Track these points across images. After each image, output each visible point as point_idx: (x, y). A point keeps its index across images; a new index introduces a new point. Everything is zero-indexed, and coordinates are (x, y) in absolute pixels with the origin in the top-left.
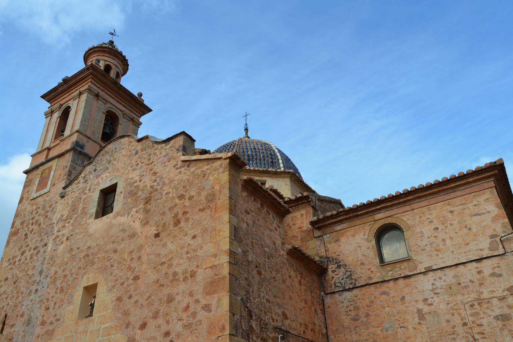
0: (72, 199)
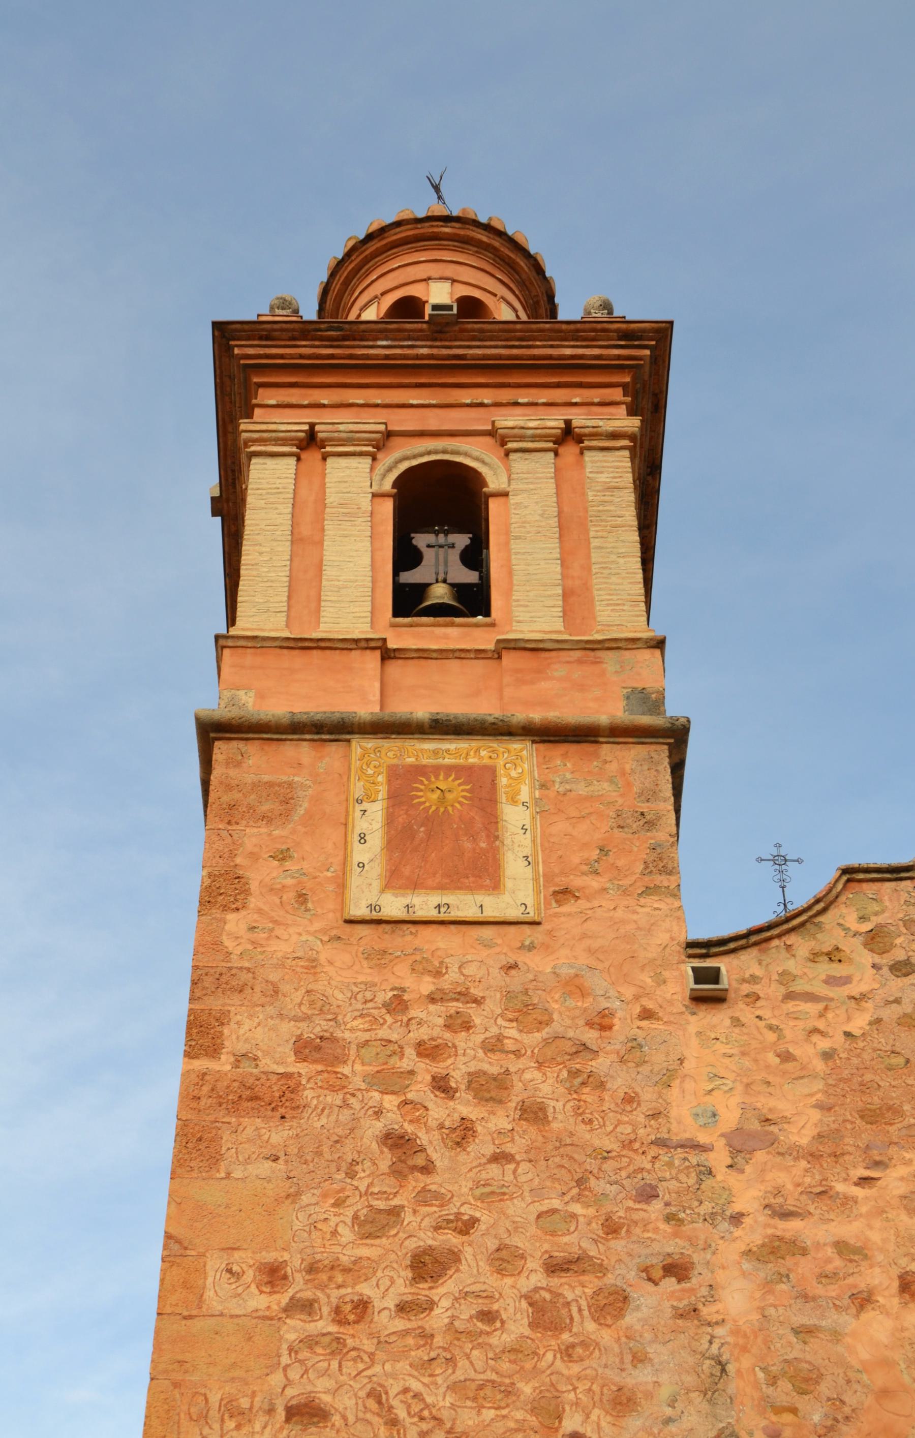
0: (824, 1044)
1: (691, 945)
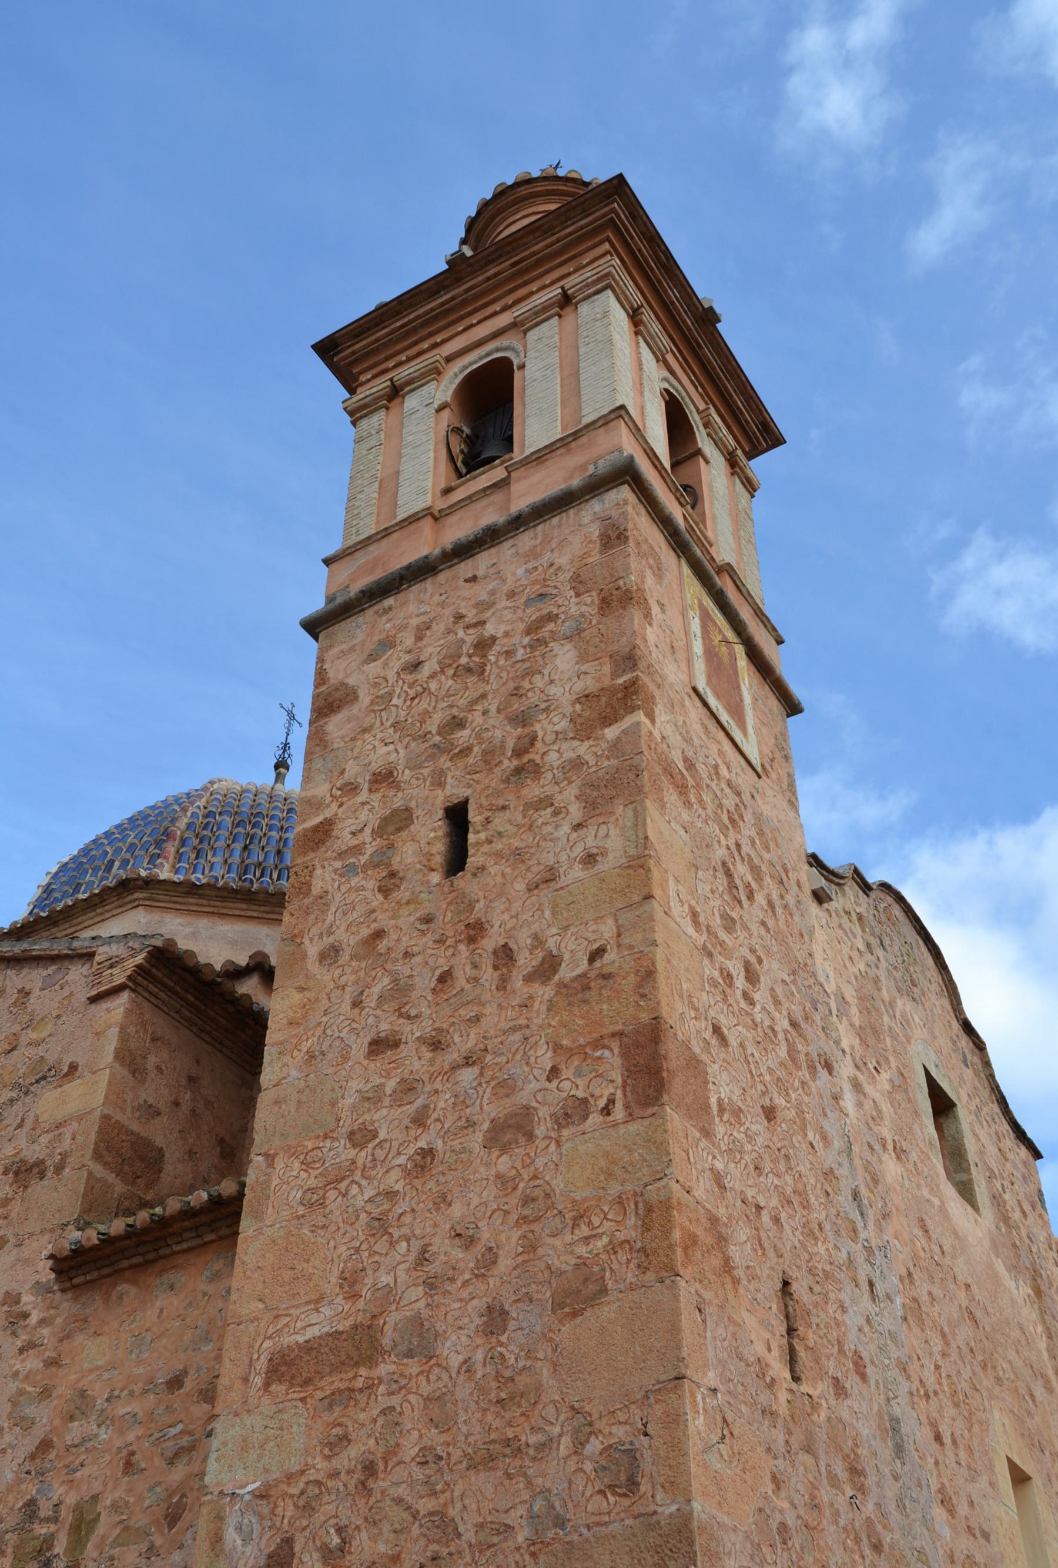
1: (814, 856)
